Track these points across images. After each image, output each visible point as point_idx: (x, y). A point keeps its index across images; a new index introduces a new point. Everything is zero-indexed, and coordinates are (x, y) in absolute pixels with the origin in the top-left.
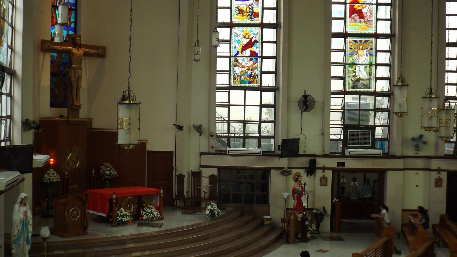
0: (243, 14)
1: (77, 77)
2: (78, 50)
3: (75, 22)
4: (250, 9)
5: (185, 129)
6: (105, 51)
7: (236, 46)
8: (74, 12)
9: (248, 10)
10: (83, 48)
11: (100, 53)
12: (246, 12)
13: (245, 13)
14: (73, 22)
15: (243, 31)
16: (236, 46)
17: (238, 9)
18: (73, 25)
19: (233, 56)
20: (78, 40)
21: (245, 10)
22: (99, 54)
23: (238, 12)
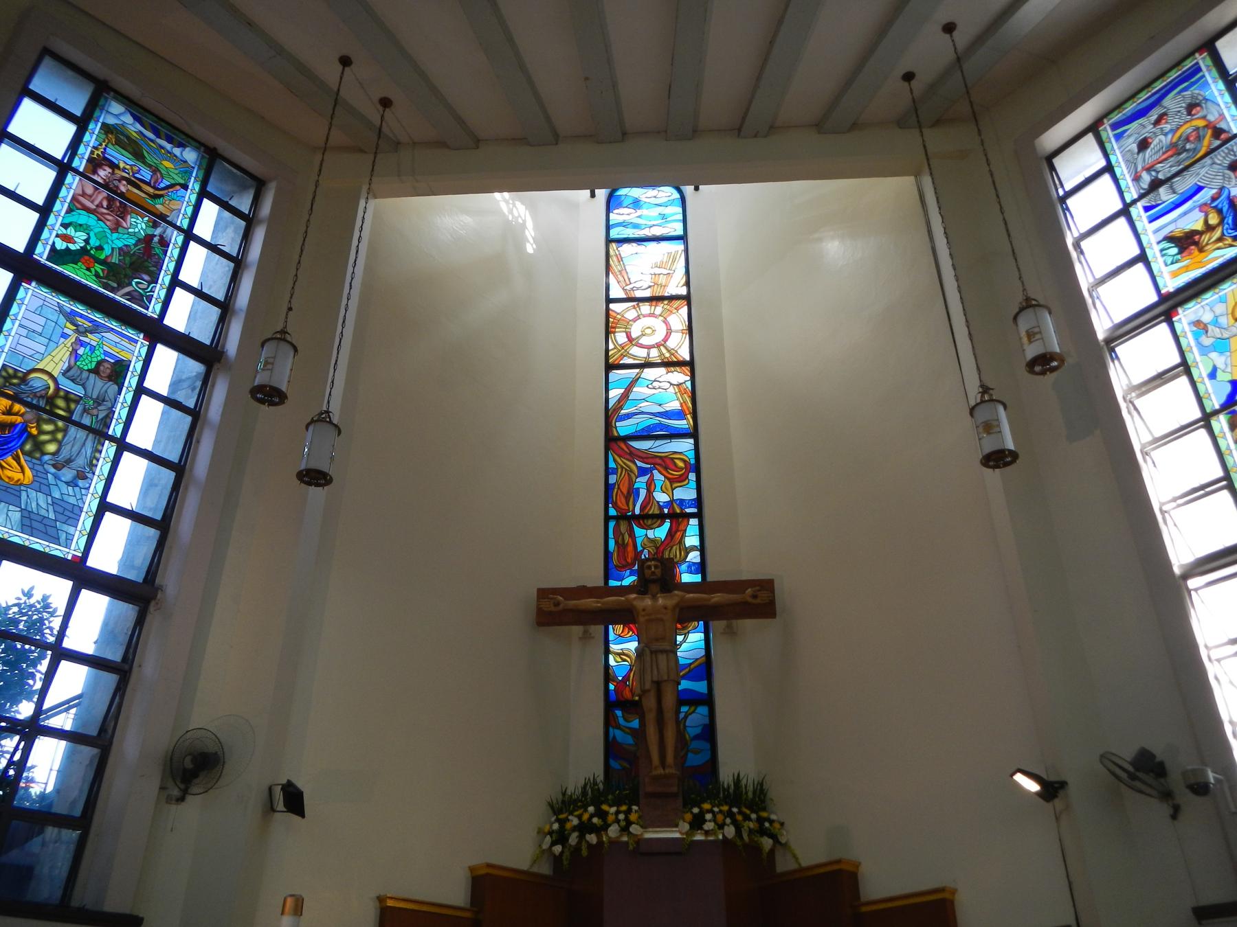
0: (1196, 244)
1: (648, 678)
2: (654, 597)
3: (702, 549)
4: (1220, 212)
5: (1073, 789)
6: (773, 591)
7: (1215, 370)
8: (694, 522)
9: (1214, 219)
11: (750, 600)
12: (1209, 228)
13: (1205, 238)
14: (693, 548)
15: (1223, 300)
16: (1215, 370)
17: (1170, 239)
18: (694, 557)
19: (1216, 413)
20: (649, 567)
21: (1199, 226)
22: (746, 603)
23: (1175, 250)
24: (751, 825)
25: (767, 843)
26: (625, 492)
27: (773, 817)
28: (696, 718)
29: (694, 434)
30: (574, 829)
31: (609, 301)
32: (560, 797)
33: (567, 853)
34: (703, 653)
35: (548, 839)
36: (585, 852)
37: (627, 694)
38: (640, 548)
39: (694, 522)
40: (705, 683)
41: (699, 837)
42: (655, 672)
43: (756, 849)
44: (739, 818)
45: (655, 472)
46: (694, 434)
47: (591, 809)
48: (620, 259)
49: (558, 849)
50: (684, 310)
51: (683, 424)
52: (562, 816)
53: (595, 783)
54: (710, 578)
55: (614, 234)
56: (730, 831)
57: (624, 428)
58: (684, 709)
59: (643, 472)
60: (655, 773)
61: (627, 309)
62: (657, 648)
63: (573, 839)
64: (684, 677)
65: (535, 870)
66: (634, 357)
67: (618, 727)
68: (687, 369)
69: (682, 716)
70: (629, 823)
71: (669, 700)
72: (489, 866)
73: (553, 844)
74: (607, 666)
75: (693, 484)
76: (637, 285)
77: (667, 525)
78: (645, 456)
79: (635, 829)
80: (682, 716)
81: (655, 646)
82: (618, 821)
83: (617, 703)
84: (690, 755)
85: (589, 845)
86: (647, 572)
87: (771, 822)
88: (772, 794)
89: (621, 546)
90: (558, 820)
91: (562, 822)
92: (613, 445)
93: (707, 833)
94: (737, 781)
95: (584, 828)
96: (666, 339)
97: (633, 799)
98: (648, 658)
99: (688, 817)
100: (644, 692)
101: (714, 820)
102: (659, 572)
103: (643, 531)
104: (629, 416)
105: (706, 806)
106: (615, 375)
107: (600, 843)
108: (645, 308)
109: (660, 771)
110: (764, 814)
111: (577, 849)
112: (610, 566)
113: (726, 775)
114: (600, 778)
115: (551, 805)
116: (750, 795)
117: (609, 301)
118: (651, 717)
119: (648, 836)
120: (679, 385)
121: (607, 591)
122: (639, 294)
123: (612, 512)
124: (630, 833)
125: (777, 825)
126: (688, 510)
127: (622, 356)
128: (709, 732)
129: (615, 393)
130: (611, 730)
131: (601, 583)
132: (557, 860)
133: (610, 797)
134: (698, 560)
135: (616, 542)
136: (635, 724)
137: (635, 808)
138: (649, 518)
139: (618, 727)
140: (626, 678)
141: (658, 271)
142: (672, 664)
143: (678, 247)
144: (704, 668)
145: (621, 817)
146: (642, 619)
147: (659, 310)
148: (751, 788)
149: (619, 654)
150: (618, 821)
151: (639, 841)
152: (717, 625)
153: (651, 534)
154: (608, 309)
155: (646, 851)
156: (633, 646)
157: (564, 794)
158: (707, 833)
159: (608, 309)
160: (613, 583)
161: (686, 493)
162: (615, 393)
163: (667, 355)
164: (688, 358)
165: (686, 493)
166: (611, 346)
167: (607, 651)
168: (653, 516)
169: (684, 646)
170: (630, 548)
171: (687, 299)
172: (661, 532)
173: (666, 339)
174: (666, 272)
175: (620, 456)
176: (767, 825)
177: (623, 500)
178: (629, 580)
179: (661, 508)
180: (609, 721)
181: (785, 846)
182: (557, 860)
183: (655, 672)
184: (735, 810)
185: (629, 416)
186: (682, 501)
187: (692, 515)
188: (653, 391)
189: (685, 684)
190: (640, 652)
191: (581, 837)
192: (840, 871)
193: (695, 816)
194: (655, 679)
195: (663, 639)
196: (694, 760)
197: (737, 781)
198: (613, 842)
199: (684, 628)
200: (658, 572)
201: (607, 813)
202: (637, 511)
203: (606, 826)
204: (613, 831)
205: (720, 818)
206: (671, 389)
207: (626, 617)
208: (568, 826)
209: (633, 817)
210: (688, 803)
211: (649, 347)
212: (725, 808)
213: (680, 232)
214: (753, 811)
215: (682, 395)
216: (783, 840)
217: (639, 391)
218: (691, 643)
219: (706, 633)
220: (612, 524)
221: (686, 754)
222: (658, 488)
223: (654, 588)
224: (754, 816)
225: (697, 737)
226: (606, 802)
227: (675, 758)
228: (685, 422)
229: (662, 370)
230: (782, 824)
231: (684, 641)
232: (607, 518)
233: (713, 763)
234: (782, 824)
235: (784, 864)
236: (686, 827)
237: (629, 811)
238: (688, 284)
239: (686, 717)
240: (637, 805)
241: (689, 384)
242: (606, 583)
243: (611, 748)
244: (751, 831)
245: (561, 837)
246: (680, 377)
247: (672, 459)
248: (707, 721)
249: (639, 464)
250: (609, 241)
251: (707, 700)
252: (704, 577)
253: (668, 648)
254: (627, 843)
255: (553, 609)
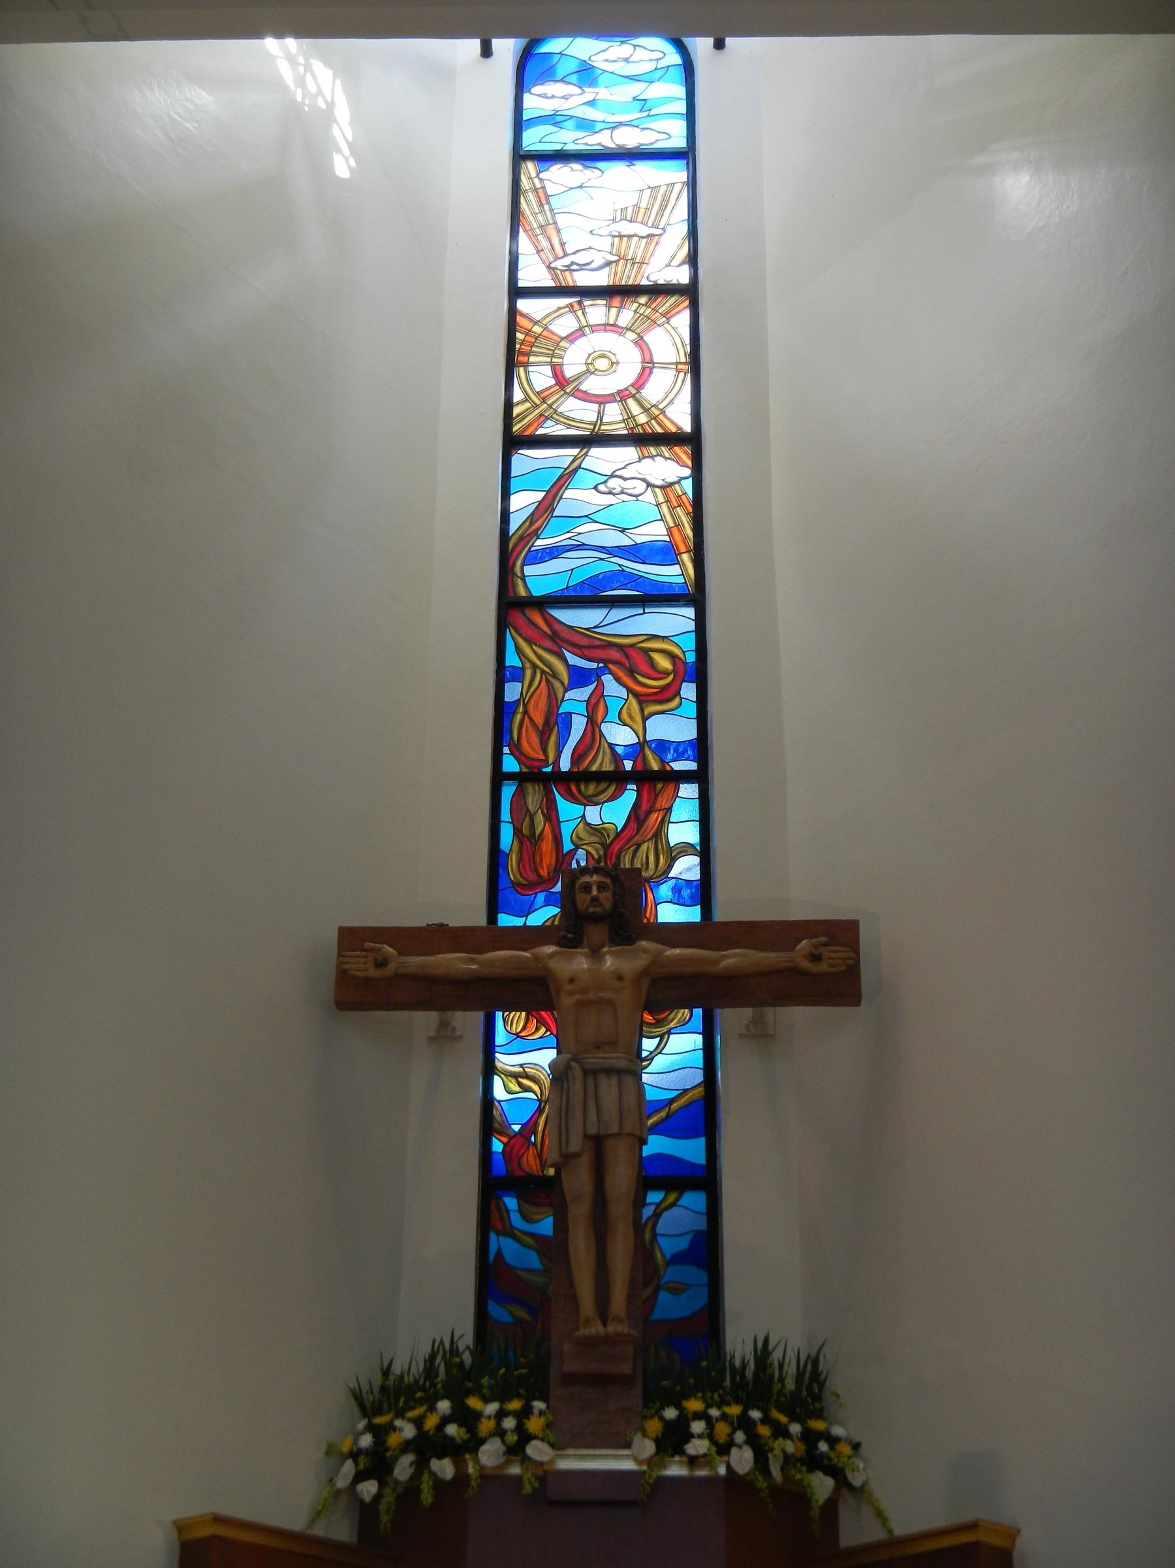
2: (595, 954)
3: (705, 851)
6: (855, 947)
8: (689, 790)
10: (644, 943)
11: (806, 964)
14: (685, 849)
18: (687, 867)
20: (587, 888)
22: (796, 971)
24: (790, 1447)
25: (821, 1485)
26: (539, 720)
27: (838, 1431)
28: (680, 1216)
29: (695, 596)
30: (406, 1446)
31: (516, 292)
32: (377, 1380)
33: (389, 1498)
34: (699, 1077)
35: (349, 1467)
36: (427, 1496)
37: (530, 1162)
38: (568, 846)
39: (689, 790)
40: (701, 1142)
41: (676, 1470)
42: (592, 1116)
43: (800, 1497)
44: (764, 1431)
45: (607, 679)
46: (695, 596)
47: (444, 1406)
48: (544, 198)
49: (369, 1488)
50: (683, 320)
51: (670, 574)
52: (378, 1420)
53: (454, 1351)
54: (719, 916)
55: (532, 140)
56: (743, 1459)
57: (540, 578)
58: (654, 1197)
59: (579, 678)
60: (584, 1332)
61: (557, 313)
62: (597, 1065)
63: (403, 1468)
64: (656, 1129)
65: (319, 1531)
66: (569, 421)
67: (509, 1231)
68: (684, 453)
69: (648, 1212)
70: (525, 1437)
71: (621, 1178)
72: (217, 1519)
73: (360, 1477)
74: (488, 1100)
75: (690, 709)
76: (580, 259)
77: (630, 796)
78: (586, 643)
79: (537, 1450)
80: (648, 1212)
81: (595, 1059)
82: (501, 1433)
83: (505, 1181)
84: (663, 1295)
85: (439, 1484)
86: (582, 900)
87: (833, 1441)
88: (838, 1382)
89: (527, 840)
90: (371, 1428)
91: (381, 1433)
92: (517, 617)
93: (693, 1461)
94: (763, 1354)
95: (427, 1446)
96: (639, 384)
97: (535, 1387)
98: (577, 1086)
99: (654, 1426)
100: (567, 1158)
101: (710, 1435)
102: (608, 900)
103: (577, 810)
104: (552, 553)
105: (694, 1405)
106: (525, 460)
107: (462, 1478)
108: (597, 311)
109: (597, 1328)
110: (818, 1425)
111: (411, 1490)
112: (503, 883)
113: (738, 1342)
114: (467, 1339)
115: (357, 1396)
116: (790, 1384)
117: (516, 292)
118: (579, 1212)
119: (568, 1464)
120: (666, 487)
121: (494, 937)
122: (584, 279)
123: (510, 764)
124: (525, 1459)
125: (845, 1449)
126: (678, 766)
127: (543, 418)
128: (706, 1249)
129: (523, 502)
130: (493, 1236)
131: (481, 920)
132: (367, 1512)
133: (485, 1381)
134: (695, 875)
135: (517, 832)
136: (546, 1226)
137: (539, 1405)
138: (587, 782)
139: (509, 1231)
140: (529, 1127)
141: (626, 228)
142: (630, 1099)
143: (676, 173)
144: (701, 1112)
145: (509, 1423)
146: (567, 1001)
147: (626, 317)
148: (791, 1370)
149: (515, 1076)
150: (501, 1433)
151: (545, 1476)
152: (732, 1018)
153: (593, 815)
154: (513, 312)
155: (557, 1497)
156: (545, 1057)
157: (386, 1373)
158: (693, 1461)
159: (513, 312)
160: (505, 920)
161: (674, 726)
162: (523, 502)
163: (642, 419)
164: (687, 427)
165: (674, 726)
166: (518, 395)
167: (490, 1069)
168: (600, 777)
169: (659, 1063)
170: (547, 846)
171: (690, 292)
172: (615, 812)
173: (639, 384)
174: (644, 231)
175: (529, 642)
176: (823, 1447)
177: (535, 739)
178: (543, 915)
179: (617, 759)
180: (489, 1218)
181: (860, 1492)
182: (367, 1512)
183: (592, 1116)
184: (755, 1414)
185: (552, 553)
186: (662, 746)
187: (686, 777)
188: (610, 499)
189: (656, 1145)
190: (559, 1073)
191: (421, 1464)
192: (974, 1547)
193: (668, 1425)
194: (592, 1130)
195: (613, 1044)
196: (669, 1306)
197: (763, 1354)
198: (487, 1477)
199: (659, 1023)
200: (606, 898)
201: (477, 1415)
202: (565, 765)
203: (474, 1443)
204: (490, 1453)
205: (722, 1429)
206: (649, 496)
207: (532, 994)
208: (393, 1440)
209: (534, 1425)
210: (655, 1398)
211: (602, 400)
212: (735, 1410)
213: (679, 141)
214: (794, 1418)
215: (672, 509)
216: (857, 1481)
217: (577, 497)
218: (673, 1057)
219: (708, 1033)
220: (508, 791)
221: (654, 1296)
222: (613, 715)
223: (597, 933)
224: (795, 1428)
225: (678, 1258)
226: (477, 1391)
227: (631, 1298)
228: (676, 569)
229: (629, 453)
230: (856, 1446)
231: (658, 1050)
232: (499, 777)
233: (712, 1316)
234: (856, 1446)
235: (856, 1530)
236: (648, 1448)
237: (523, 1415)
238: (693, 259)
239: (657, 1215)
240: (544, 1398)
241: (688, 486)
242: (492, 919)
243: (492, 1278)
244: (788, 1460)
245: (376, 1464)
246: (668, 468)
247: (646, 651)
248: (702, 1224)
249: (573, 660)
250: (520, 156)
251: (705, 1178)
252: (707, 912)
253: (623, 1064)
254: (519, 1479)
255: (372, 972)
